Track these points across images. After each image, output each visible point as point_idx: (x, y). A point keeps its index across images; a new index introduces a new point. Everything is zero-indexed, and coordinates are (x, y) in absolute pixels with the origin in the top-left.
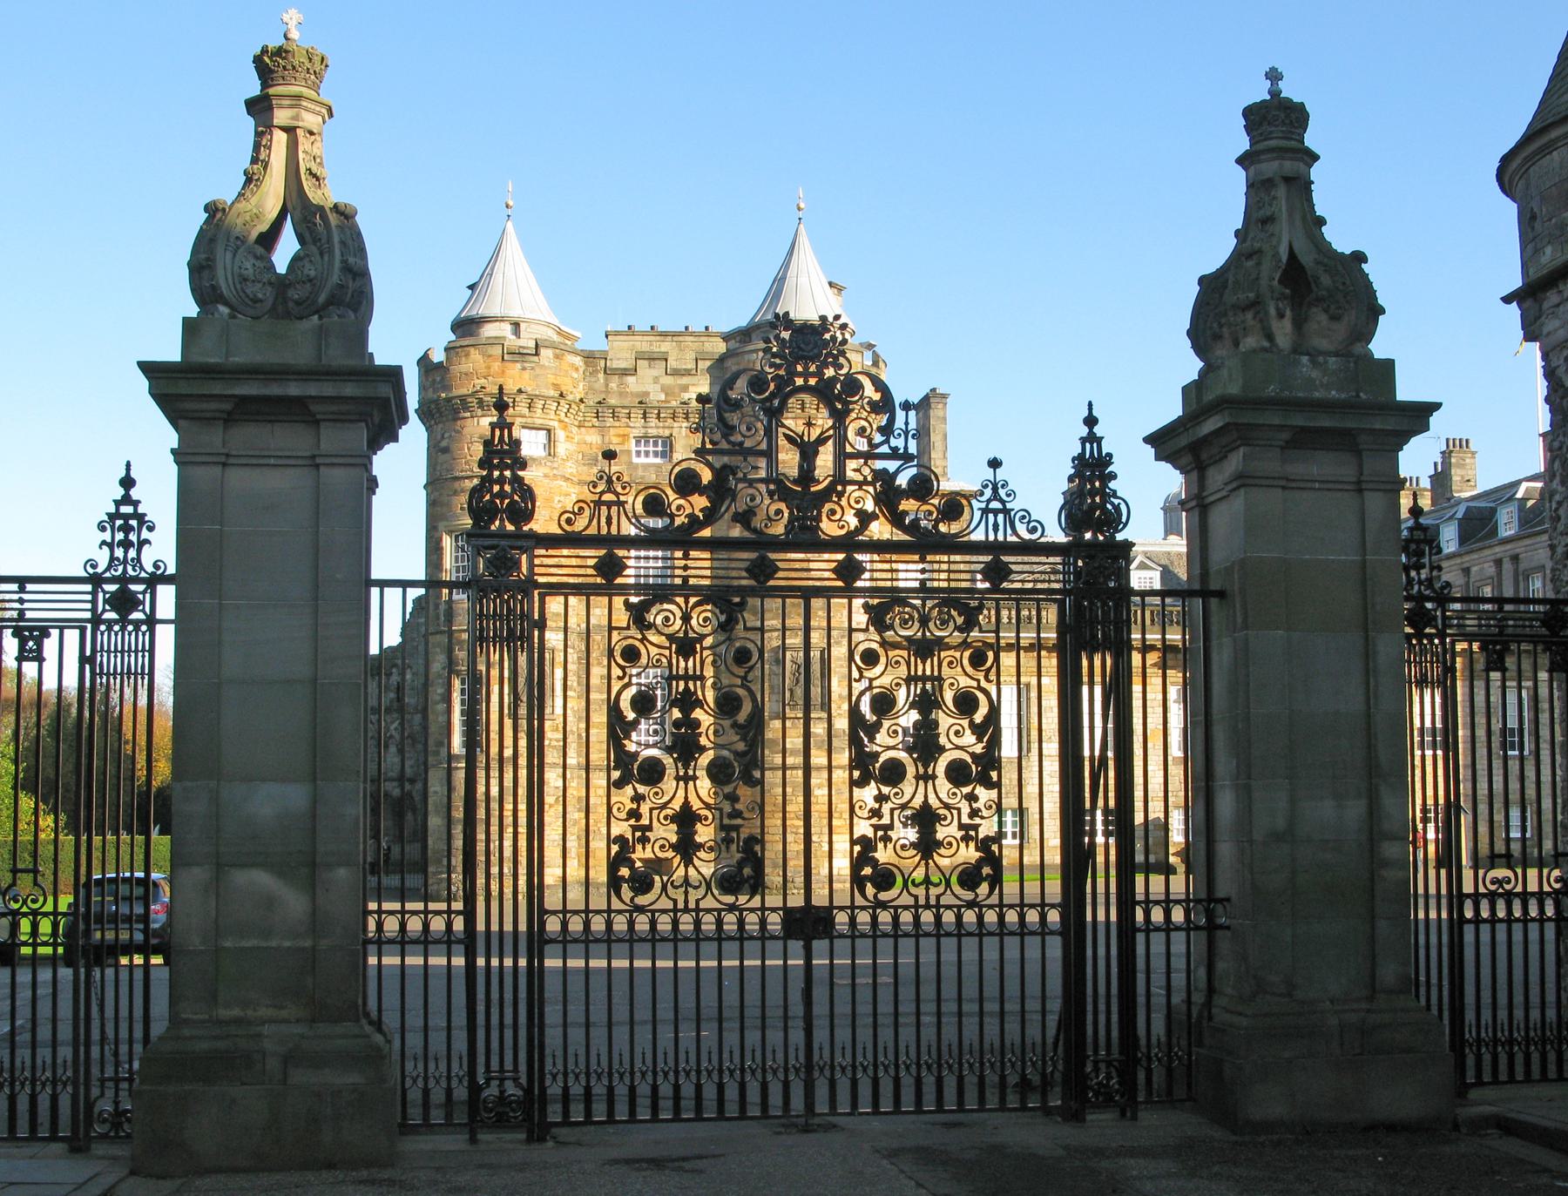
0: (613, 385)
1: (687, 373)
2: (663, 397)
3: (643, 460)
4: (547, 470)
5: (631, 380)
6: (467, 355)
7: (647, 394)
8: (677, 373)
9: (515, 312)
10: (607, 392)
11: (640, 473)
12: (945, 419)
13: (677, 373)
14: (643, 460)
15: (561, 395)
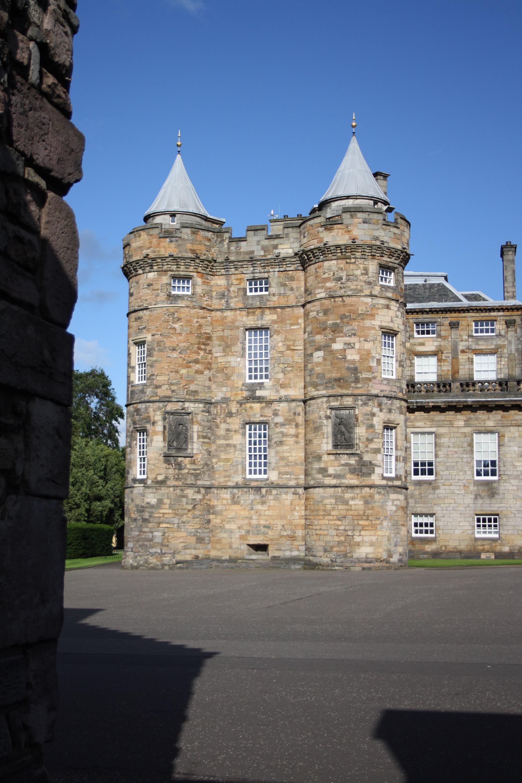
0: (233, 248)
1: (278, 237)
2: (262, 253)
3: (254, 293)
4: (188, 303)
5: (243, 244)
6: (140, 236)
7: (253, 252)
8: (270, 238)
9: (175, 208)
10: (229, 253)
11: (250, 302)
12: (513, 261)
13: (270, 238)
14: (254, 293)
15: (198, 258)
